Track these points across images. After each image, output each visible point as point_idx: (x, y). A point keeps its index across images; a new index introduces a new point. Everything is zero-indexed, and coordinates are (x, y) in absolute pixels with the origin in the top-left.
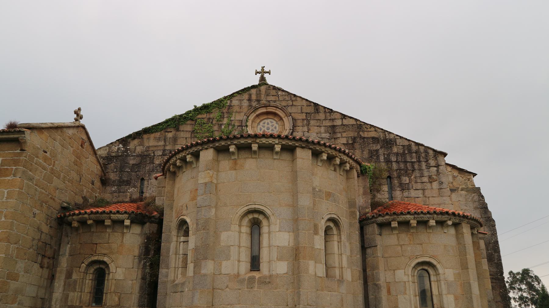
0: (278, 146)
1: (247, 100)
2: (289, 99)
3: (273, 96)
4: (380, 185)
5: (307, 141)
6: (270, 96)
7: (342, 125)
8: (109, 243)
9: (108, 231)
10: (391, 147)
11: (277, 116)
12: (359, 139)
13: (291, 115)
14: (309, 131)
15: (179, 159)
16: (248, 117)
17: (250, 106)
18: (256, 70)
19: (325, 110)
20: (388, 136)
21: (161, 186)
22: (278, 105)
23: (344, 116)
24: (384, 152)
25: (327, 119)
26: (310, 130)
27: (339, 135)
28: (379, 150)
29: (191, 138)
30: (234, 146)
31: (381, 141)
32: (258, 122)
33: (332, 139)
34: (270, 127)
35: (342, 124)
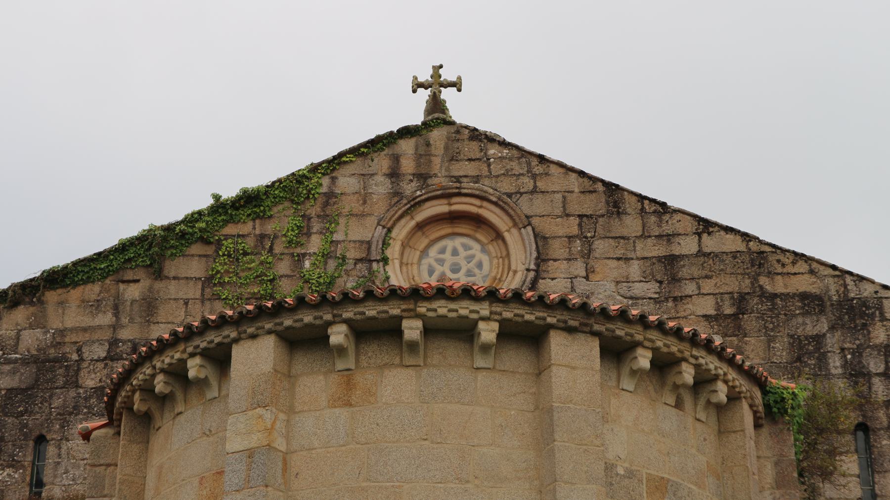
0: (489, 328)
1: (385, 175)
2: (524, 171)
3: (470, 160)
4: (833, 453)
5: (584, 307)
6: (461, 160)
7: (700, 253)
10: (864, 326)
11: (483, 226)
12: (756, 300)
13: (530, 224)
14: (591, 276)
15: (162, 371)
16: (389, 230)
17: (397, 194)
18: (415, 78)
19: (643, 204)
20: (855, 288)
21: (102, 462)
22: (486, 192)
23: (705, 226)
24: (844, 341)
25: (650, 236)
26: (593, 272)
27: (690, 288)
28: (824, 335)
29: (203, 302)
30: (343, 328)
31: (832, 305)
32: (422, 246)
33: (667, 299)
34: (463, 263)
35: (699, 251)
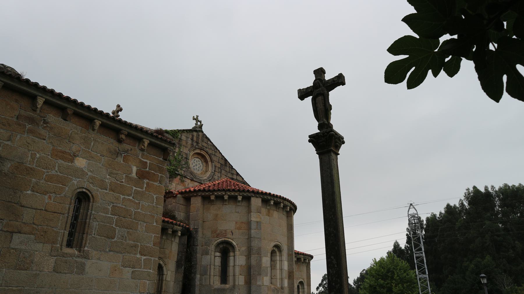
1: (190, 139)
2: (213, 150)
8: (164, 248)
9: (163, 237)
23: (238, 174)
25: (230, 173)
